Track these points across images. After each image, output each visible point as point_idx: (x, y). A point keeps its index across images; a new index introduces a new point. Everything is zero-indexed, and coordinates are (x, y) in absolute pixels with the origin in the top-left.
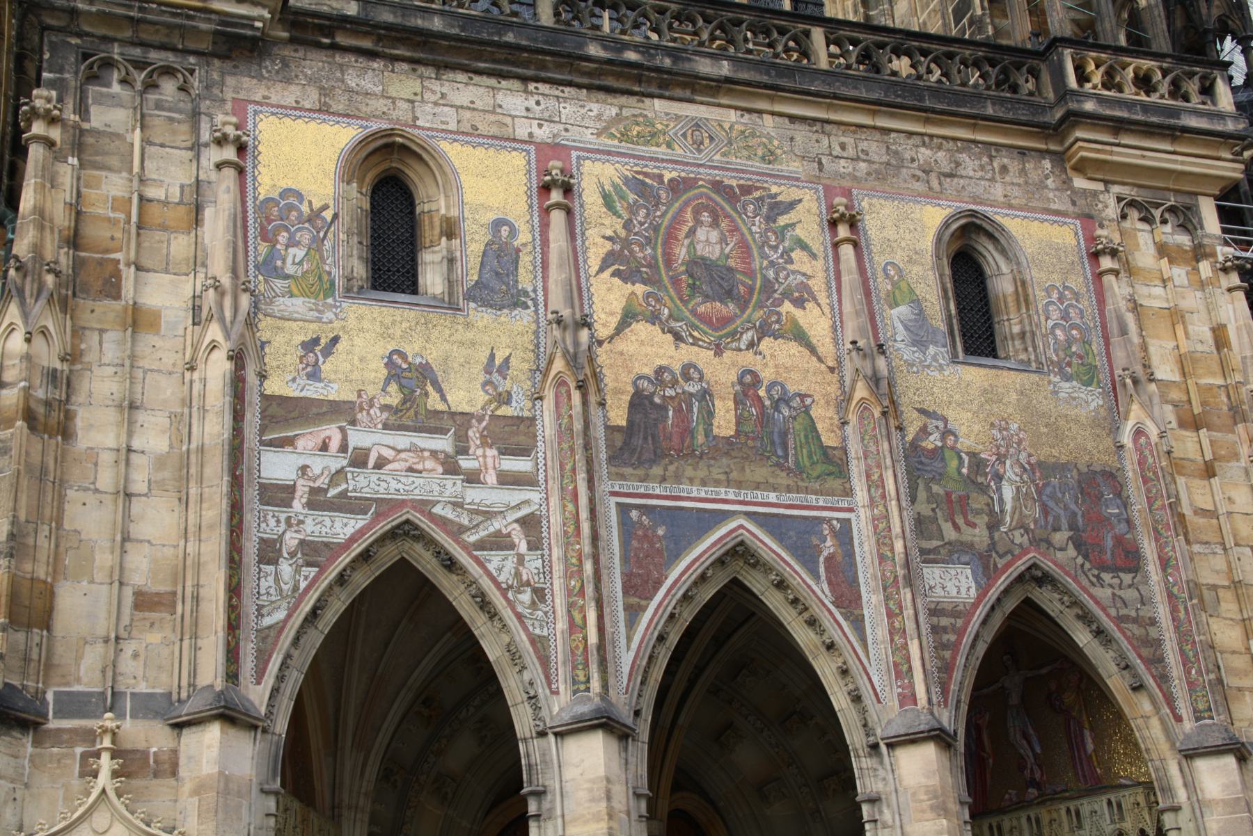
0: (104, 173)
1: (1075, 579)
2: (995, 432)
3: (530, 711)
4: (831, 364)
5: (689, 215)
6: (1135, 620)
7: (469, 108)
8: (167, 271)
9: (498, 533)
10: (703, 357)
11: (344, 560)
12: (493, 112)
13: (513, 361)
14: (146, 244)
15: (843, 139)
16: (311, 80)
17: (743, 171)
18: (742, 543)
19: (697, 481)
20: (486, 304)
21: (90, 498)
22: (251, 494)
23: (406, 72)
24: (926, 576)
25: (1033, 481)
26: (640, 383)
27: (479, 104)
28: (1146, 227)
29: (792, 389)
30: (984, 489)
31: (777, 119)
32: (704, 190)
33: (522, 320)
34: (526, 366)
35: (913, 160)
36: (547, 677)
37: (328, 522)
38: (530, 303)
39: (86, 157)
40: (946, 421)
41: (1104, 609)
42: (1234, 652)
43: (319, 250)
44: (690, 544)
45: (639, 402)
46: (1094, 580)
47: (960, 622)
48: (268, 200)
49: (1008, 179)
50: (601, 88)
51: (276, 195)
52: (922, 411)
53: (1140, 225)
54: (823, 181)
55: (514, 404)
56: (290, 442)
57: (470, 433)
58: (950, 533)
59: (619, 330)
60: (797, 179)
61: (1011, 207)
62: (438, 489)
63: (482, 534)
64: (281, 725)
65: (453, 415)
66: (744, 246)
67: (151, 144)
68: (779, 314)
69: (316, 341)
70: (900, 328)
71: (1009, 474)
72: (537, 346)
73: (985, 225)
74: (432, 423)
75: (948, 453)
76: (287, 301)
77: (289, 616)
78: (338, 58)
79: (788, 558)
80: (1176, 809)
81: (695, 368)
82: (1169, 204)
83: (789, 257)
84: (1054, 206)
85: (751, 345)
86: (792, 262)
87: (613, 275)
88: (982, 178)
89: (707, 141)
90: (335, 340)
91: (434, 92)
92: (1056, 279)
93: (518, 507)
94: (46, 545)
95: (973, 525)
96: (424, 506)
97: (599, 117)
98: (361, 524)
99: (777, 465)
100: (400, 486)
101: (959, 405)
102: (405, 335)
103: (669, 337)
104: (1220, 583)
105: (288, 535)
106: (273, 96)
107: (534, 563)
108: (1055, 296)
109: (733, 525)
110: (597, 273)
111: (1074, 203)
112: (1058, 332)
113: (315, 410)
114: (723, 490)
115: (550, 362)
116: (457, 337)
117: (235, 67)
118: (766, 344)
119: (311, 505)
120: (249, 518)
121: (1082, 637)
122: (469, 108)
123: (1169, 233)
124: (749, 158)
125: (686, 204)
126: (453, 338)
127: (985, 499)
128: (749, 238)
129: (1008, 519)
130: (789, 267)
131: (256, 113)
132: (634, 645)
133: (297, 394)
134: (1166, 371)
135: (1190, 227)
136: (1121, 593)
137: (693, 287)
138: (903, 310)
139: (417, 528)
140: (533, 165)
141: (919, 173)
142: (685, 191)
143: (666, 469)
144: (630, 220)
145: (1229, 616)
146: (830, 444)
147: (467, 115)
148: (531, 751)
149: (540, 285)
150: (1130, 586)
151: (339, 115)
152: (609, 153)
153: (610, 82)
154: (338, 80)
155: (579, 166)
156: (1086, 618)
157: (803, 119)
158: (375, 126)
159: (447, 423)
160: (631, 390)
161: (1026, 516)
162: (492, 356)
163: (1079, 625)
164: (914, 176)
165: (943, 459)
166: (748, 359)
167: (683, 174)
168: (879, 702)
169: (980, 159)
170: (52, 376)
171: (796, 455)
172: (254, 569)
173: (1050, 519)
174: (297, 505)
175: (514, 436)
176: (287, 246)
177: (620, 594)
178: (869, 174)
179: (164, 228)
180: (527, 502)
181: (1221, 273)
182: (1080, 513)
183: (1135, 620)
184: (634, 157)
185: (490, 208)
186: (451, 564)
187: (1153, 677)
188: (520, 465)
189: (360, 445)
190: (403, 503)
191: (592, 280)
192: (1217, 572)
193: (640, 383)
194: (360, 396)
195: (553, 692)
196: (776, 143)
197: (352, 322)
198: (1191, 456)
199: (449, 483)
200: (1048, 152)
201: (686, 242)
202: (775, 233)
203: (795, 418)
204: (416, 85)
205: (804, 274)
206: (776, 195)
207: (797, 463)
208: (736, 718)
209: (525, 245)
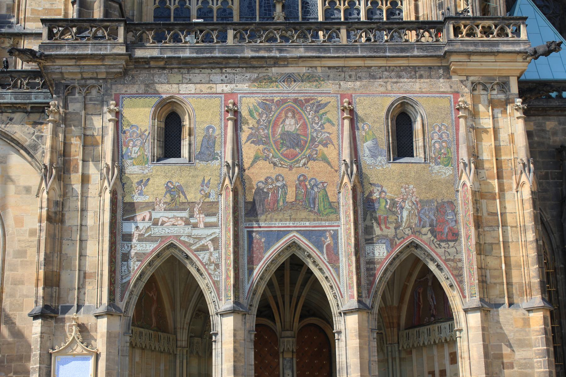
2: (403, 190)
3: (214, 306)
4: (336, 169)
5: (283, 115)
6: (453, 260)
9: (203, 245)
10: (284, 171)
11: (150, 258)
12: (209, 83)
14: (86, 152)
15: (350, 73)
16: (142, 82)
17: (307, 93)
18: (294, 242)
19: (278, 220)
20: (201, 160)
22: (119, 238)
23: (176, 73)
26: (259, 184)
28: (485, 92)
29: (319, 180)
30: (394, 213)
31: (323, 68)
32: (290, 103)
34: (216, 182)
36: (218, 295)
37: (144, 246)
38: (219, 158)
39: (67, 123)
40: (382, 187)
41: (440, 257)
42: (495, 269)
43: (143, 147)
44: (274, 244)
46: (437, 246)
53: (482, 92)
54: (340, 93)
55: (211, 197)
57: (195, 209)
59: (252, 165)
60: (329, 93)
61: (422, 93)
62: (182, 230)
63: (198, 246)
64: (131, 313)
66: (305, 125)
67: (88, 114)
68: (316, 150)
69: (142, 181)
70: (367, 151)
71: (407, 206)
73: (409, 102)
74: (182, 207)
75: (381, 200)
78: (152, 72)
79: (311, 246)
80: (461, 330)
81: (280, 175)
82: (496, 82)
83: (323, 127)
84: (441, 90)
85: (304, 164)
87: (251, 143)
90: (148, 180)
91: (186, 79)
93: (211, 235)
94: (56, 260)
95: (389, 228)
96: (177, 237)
98: (155, 245)
99: (310, 211)
100: (169, 231)
104: (494, 242)
105: (132, 251)
106: (128, 90)
107: (216, 255)
108: (437, 129)
109: (291, 235)
111: (451, 87)
112: (436, 145)
113: (141, 206)
114: (288, 223)
116: (191, 174)
117: (116, 81)
120: (118, 246)
121: (432, 267)
122: (199, 83)
123: (497, 95)
125: (282, 110)
126: (191, 174)
128: (307, 120)
129: (404, 224)
130: (323, 131)
135: (504, 90)
136: (448, 250)
137: (282, 144)
138: (369, 143)
139: (175, 245)
140: (223, 103)
142: (282, 105)
143: (266, 217)
144: (260, 120)
147: (199, 86)
149: (223, 150)
150: (452, 247)
152: (253, 93)
154: (152, 80)
156: (433, 260)
157: (334, 67)
159: (187, 206)
162: (204, 180)
165: (379, 203)
167: (282, 98)
168: (342, 297)
169: (411, 73)
170: (57, 203)
171: (318, 206)
172: (120, 264)
173: (422, 223)
175: (210, 209)
176: (132, 147)
177: (246, 264)
180: (214, 233)
181: (515, 111)
184: (263, 93)
186: (187, 257)
187: (457, 282)
188: (212, 219)
191: (243, 146)
193: (259, 184)
195: (220, 300)
200: (441, 66)
201: (281, 126)
202: (318, 117)
203: (319, 192)
205: (329, 133)
207: (318, 210)
209: (218, 135)
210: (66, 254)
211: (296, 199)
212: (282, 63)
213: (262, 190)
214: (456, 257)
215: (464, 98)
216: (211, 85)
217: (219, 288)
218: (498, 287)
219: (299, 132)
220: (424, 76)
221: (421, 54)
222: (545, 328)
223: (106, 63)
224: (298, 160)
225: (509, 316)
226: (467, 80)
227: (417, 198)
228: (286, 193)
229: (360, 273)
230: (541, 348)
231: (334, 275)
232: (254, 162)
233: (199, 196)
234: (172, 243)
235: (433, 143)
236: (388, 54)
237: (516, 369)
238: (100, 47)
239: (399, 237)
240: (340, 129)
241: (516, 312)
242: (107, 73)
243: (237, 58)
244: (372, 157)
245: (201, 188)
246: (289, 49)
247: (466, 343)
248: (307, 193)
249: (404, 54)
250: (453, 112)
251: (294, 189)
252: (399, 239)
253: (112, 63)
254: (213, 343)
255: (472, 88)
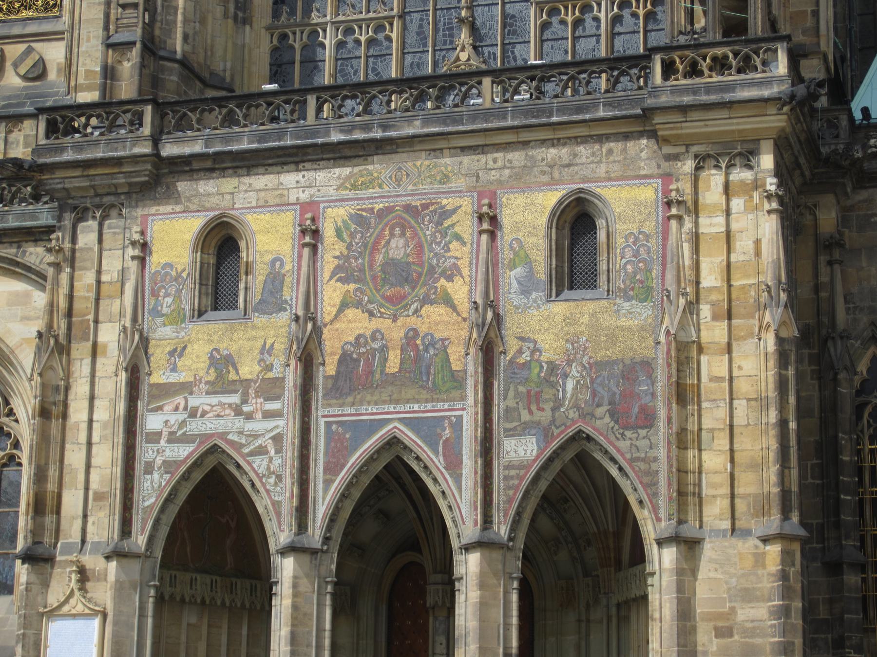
0: (83, 272)
1: (606, 438)
2: (569, 346)
4: (465, 316)
5: (387, 233)
6: (643, 460)
7: (264, 190)
8: (110, 321)
11: (183, 468)
13: (276, 345)
17: (425, 194)
18: (395, 437)
19: (372, 403)
20: (263, 312)
21: (75, 447)
23: (231, 176)
24: (505, 445)
25: (589, 375)
26: (346, 347)
27: (270, 186)
29: (437, 336)
30: (553, 385)
33: (284, 318)
34: (283, 347)
35: (543, 160)
37: (176, 450)
38: (288, 307)
39: (77, 265)
40: (535, 342)
41: (622, 455)
42: (716, 472)
43: (180, 297)
44: (364, 442)
45: (345, 359)
46: (619, 436)
47: (522, 472)
48: (156, 272)
49: (611, 158)
50: (340, 158)
51: (159, 269)
52: (517, 338)
53: (714, 172)
54: (478, 189)
56: (160, 408)
58: (525, 416)
59: (337, 316)
60: (461, 192)
61: (610, 179)
63: (252, 447)
64: (159, 554)
65: (241, 381)
68: (436, 288)
69: (175, 350)
71: (574, 372)
72: (289, 334)
75: (533, 364)
76: (163, 329)
77: (156, 500)
81: (378, 331)
82: (736, 151)
84: (643, 172)
85: (416, 311)
86: (449, 250)
88: (592, 162)
89: (404, 178)
90: (185, 347)
91: (245, 184)
92: (634, 228)
93: (272, 430)
95: (543, 410)
96: (223, 435)
97: (339, 177)
98: (192, 449)
99: (421, 387)
100: (213, 426)
101: (546, 330)
102: (219, 341)
103: (366, 314)
105: (158, 459)
108: (632, 240)
110: (328, 281)
111: (659, 167)
112: (629, 267)
113: (173, 389)
115: (292, 344)
116: (247, 335)
117: (143, 195)
118: (427, 309)
119: (169, 441)
121: (614, 472)
124: (431, 183)
125: (386, 225)
127: (552, 391)
128: (423, 239)
129: (567, 403)
130: (448, 254)
131: (153, 221)
132: (326, 502)
133: (165, 381)
134: (710, 278)
136: (637, 443)
137: (384, 280)
138: (519, 271)
141: (546, 169)
142: (386, 216)
144: (351, 243)
145: (719, 448)
146: (457, 368)
147: (263, 194)
148: (276, 560)
149: (294, 295)
150: (644, 438)
151: (194, 212)
152: (343, 200)
153: (348, 153)
155: (324, 212)
156: (613, 460)
158: (212, 214)
159: (238, 386)
160: (340, 352)
161: (580, 399)
162: (265, 343)
163: (612, 464)
164: (542, 171)
165: (530, 369)
166: (413, 321)
167: (387, 204)
168: (464, 523)
171: (434, 381)
173: (596, 399)
174: (162, 442)
175: (271, 389)
177: (321, 475)
178: (510, 177)
179: (110, 297)
180: (277, 427)
182: (618, 392)
183: (643, 460)
184: (358, 199)
185: (270, 252)
187: (648, 495)
188: (274, 406)
189: (194, 405)
190: (212, 435)
192: (717, 420)
193: (346, 347)
194: (195, 378)
196: (450, 169)
197: (193, 336)
198: (716, 340)
199: (237, 421)
201: (383, 250)
202: (441, 233)
203: (436, 355)
204: (235, 181)
205: (456, 258)
206: (445, 206)
207: (434, 383)
208: (390, 537)
209: (288, 271)
210: (70, 465)
212: (389, 147)
213: (350, 355)
214: (648, 455)
215: (679, 185)
216: (280, 192)
217: (280, 512)
218: (718, 502)
219: (410, 259)
220: (615, 151)
221: (610, 114)
222: (783, 571)
223: (124, 170)
224: (407, 304)
225: (731, 551)
226: (687, 151)
227: (590, 358)
228: (386, 360)
229: (491, 484)
230: (776, 603)
231: (453, 488)
232: (340, 311)
233: (257, 368)
234: (215, 445)
235: (622, 264)
236: (555, 119)
237: (736, 637)
238: (116, 145)
239: (558, 423)
240: (475, 251)
241: (744, 543)
242: (130, 184)
243: (315, 145)
244: (522, 294)
245: (258, 358)
246: (398, 124)
247: (657, 596)
248: (418, 359)
249: (581, 117)
250: (660, 209)
252: (557, 428)
253: (132, 169)
254: (273, 598)
255: (694, 166)
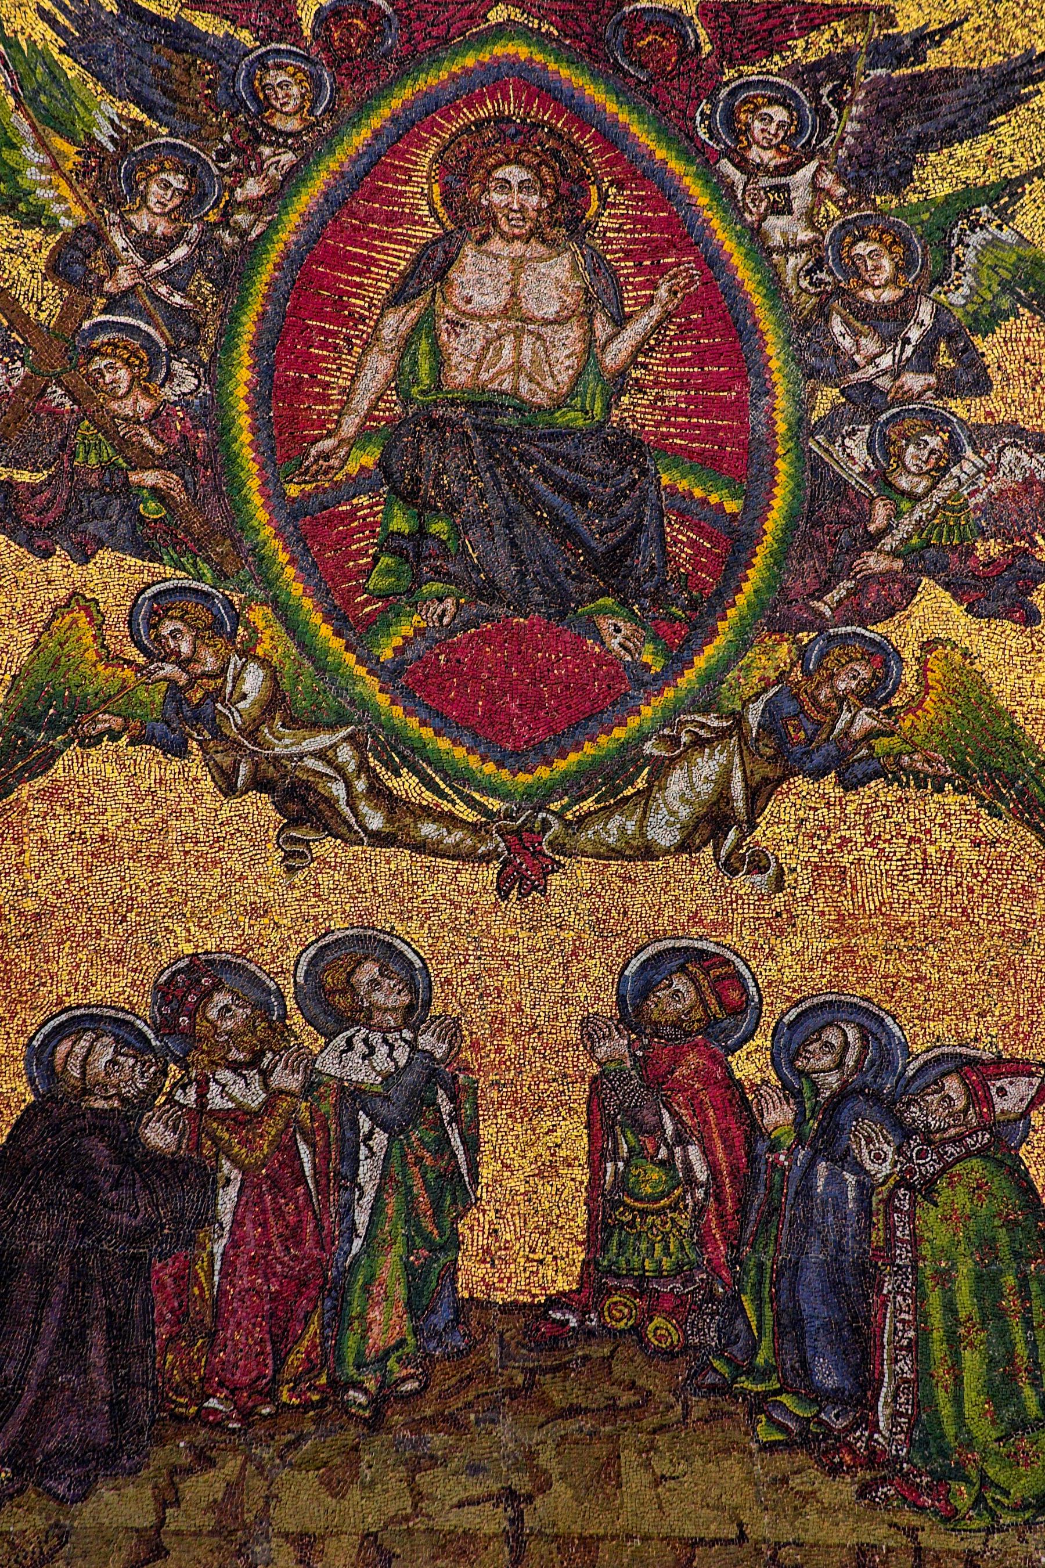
10: (436, 904)
29: (922, 1035)
211: (595, 1282)
251: (572, 1134)
